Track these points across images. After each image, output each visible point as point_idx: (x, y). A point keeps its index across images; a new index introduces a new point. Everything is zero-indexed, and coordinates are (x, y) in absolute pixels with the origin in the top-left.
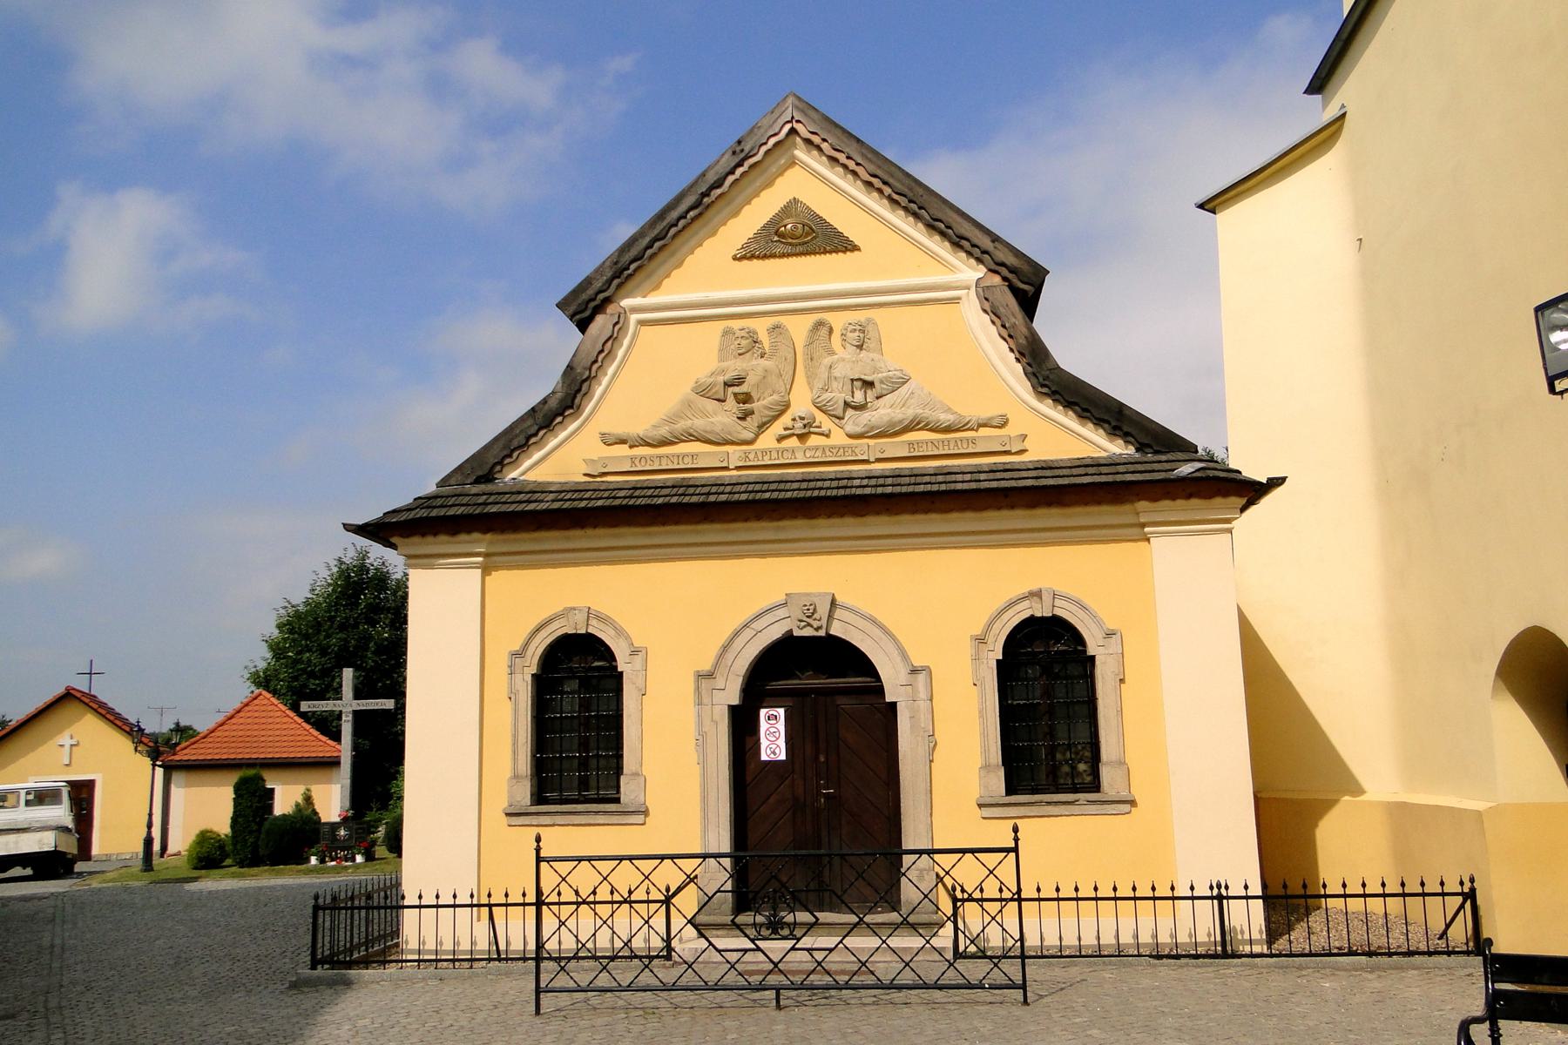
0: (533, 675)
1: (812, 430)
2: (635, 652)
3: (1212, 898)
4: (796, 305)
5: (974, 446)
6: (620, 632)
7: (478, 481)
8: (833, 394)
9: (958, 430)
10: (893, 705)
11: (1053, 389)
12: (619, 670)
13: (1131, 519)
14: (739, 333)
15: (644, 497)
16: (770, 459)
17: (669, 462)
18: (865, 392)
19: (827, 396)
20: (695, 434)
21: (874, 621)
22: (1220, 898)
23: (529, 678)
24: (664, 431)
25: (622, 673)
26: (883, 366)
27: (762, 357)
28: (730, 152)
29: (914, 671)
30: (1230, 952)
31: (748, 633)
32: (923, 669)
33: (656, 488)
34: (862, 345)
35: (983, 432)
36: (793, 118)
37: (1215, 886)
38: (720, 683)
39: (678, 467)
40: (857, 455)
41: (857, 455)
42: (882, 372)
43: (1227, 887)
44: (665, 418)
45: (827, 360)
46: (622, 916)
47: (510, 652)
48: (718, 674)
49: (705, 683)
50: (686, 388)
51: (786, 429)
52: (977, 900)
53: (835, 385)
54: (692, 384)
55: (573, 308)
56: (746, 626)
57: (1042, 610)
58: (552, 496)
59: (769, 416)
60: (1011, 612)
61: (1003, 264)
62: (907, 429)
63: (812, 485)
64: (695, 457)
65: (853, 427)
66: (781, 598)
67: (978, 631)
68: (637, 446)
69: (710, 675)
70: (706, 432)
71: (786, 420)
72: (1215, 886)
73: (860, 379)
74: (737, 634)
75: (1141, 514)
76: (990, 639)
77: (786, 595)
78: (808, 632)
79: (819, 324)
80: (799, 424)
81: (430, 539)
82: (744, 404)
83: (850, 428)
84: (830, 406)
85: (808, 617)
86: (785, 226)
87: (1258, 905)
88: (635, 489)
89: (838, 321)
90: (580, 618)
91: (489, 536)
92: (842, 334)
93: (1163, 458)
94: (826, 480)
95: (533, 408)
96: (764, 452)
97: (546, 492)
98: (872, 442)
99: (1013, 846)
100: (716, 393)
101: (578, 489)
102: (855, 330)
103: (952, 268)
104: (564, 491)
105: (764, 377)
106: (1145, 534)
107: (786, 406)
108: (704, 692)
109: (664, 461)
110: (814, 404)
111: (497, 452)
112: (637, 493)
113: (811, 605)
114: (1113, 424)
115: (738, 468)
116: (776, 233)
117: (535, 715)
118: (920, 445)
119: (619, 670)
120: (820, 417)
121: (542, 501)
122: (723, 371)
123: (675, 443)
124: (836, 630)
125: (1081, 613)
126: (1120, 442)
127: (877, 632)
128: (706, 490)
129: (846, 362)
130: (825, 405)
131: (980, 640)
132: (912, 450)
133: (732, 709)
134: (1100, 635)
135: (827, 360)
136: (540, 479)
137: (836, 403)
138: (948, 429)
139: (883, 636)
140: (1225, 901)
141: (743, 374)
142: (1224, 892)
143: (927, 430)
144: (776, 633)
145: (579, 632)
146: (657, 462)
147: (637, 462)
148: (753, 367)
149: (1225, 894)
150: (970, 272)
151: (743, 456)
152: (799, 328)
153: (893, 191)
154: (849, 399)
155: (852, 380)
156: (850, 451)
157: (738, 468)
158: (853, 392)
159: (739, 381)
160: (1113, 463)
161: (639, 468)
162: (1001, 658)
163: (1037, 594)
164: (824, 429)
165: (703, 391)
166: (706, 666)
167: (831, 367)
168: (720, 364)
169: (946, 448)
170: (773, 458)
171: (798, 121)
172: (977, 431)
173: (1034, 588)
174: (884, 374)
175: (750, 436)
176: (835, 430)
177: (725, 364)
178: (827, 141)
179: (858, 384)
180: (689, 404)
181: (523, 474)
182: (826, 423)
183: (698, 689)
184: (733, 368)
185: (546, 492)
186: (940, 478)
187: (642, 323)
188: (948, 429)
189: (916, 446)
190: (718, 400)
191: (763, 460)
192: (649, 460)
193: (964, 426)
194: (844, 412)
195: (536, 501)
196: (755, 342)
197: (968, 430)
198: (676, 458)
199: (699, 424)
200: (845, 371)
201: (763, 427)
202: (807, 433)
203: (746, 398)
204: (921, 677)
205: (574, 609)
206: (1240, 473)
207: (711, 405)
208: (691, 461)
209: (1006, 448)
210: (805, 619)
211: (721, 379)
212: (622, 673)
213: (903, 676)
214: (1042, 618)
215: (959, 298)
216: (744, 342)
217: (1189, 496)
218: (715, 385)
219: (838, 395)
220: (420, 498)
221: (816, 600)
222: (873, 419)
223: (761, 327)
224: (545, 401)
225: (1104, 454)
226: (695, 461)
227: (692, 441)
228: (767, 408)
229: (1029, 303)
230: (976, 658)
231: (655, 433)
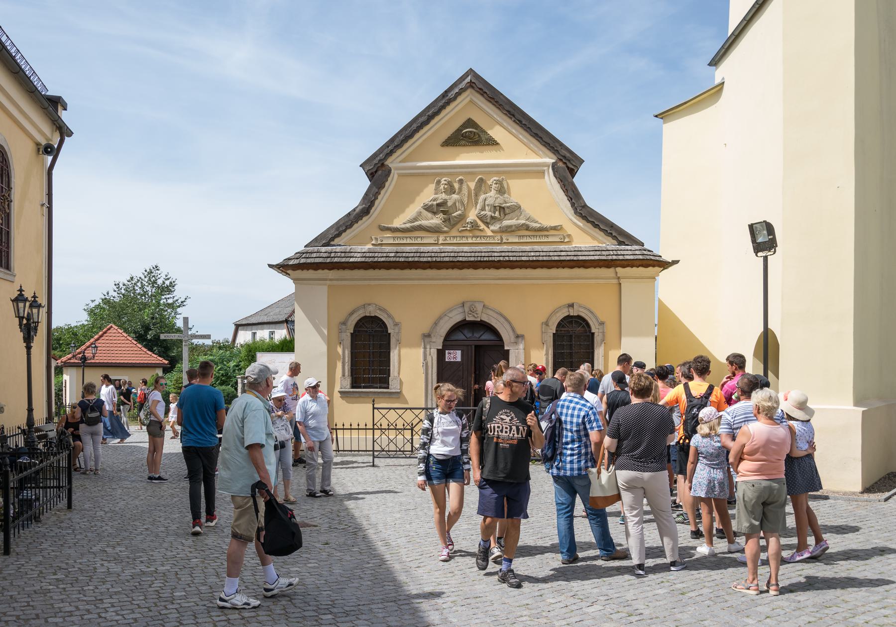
2: (396, 324)
4: (470, 171)
6: (389, 316)
7: (323, 246)
12: (389, 332)
19: (483, 213)
21: (502, 315)
23: (349, 335)
24: (408, 225)
25: (390, 334)
28: (442, 96)
29: (518, 337)
31: (446, 318)
38: (434, 339)
46: (392, 434)
48: (432, 335)
49: (427, 340)
53: (487, 208)
54: (422, 205)
55: (368, 168)
57: (573, 313)
61: (564, 157)
63: (477, 254)
67: (545, 320)
74: (440, 318)
79: (481, 181)
95: (349, 213)
110: (478, 217)
111: (333, 232)
112: (398, 255)
115: (442, 244)
119: (389, 332)
120: (480, 223)
122: (434, 200)
124: (485, 319)
125: (590, 315)
127: (502, 320)
128: (429, 255)
129: (492, 196)
131: (546, 324)
150: (550, 159)
154: (493, 215)
159: (443, 204)
163: (571, 306)
172: (548, 231)
173: (570, 302)
177: (437, 196)
180: (420, 214)
182: (482, 226)
184: (440, 198)
186: (532, 254)
199: (424, 223)
207: (430, 215)
211: (435, 203)
212: (390, 334)
213: (513, 339)
220: (299, 253)
224: (354, 210)
228: (455, 217)
229: (573, 173)
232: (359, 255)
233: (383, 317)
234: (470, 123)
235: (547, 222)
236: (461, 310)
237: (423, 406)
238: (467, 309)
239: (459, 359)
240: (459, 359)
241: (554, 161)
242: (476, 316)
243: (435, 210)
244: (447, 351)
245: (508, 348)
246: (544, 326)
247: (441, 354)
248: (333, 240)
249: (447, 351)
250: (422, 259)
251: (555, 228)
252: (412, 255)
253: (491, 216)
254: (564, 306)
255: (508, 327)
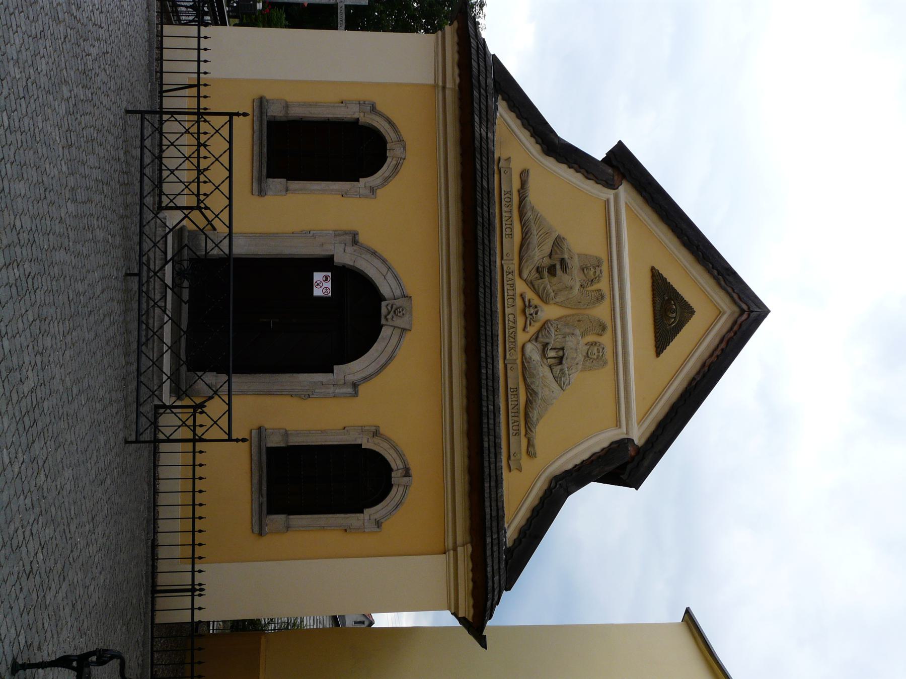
0: (358, 119)
1: (529, 320)
2: (373, 190)
3: (193, 584)
4: (618, 312)
5: (514, 434)
6: (386, 180)
8: (553, 335)
9: (526, 423)
10: (332, 371)
11: (553, 491)
13: (460, 540)
14: (598, 270)
15: (482, 198)
16: (508, 290)
17: (507, 218)
18: (555, 358)
20: (527, 236)
21: (391, 358)
22: (193, 590)
23: (356, 116)
25: (358, 181)
26: (573, 371)
27: (582, 286)
29: (355, 386)
30: (156, 595)
31: (384, 270)
32: (356, 394)
33: (489, 208)
34: (588, 357)
35: (524, 442)
36: (752, 312)
37: (202, 587)
38: (349, 249)
39: (504, 225)
40: (509, 351)
41: (509, 351)
42: (568, 370)
43: (200, 595)
44: (539, 216)
45: (578, 332)
46: (187, 176)
47: (375, 103)
48: (355, 248)
49: (348, 238)
50: (560, 229)
51: (529, 301)
52: (198, 178)
54: (563, 235)
56: (389, 268)
58: (484, 134)
59: (539, 288)
60: (395, 455)
61: (643, 458)
62: (528, 387)
64: (510, 236)
65: (529, 349)
66: (409, 291)
67: (382, 431)
68: (519, 196)
69: (355, 242)
70: (528, 244)
71: (536, 301)
72: (202, 587)
73: (564, 355)
74: (384, 261)
75: (462, 548)
76: (377, 440)
77: (411, 297)
78: (384, 311)
79: (603, 328)
80: (532, 311)
81: (456, 48)
82: (548, 272)
83: (529, 347)
84: (545, 335)
85: (395, 312)
86: (675, 305)
87: (186, 617)
88: (489, 193)
89: (606, 339)
90: (398, 152)
91: (457, 88)
92: (596, 343)
93: (503, 566)
94: (492, 328)
96: (513, 286)
97: (487, 131)
98: (519, 362)
99: (233, 438)
100: (556, 251)
101: (489, 153)
102: (599, 352)
103: (640, 422)
104: (487, 141)
105: (567, 287)
106: (449, 551)
107: (546, 302)
108: (343, 237)
109: (508, 215)
112: (485, 194)
113: (403, 314)
114: (527, 532)
115: (502, 266)
116: (670, 299)
117: (331, 120)
118: (516, 396)
121: (480, 127)
123: (521, 221)
124: (385, 332)
125: (394, 503)
126: (515, 536)
127: (383, 360)
130: (545, 329)
131: (376, 433)
132: (512, 390)
133: (331, 258)
134: (377, 516)
135: (578, 332)
136: (497, 127)
137: (547, 336)
138: (527, 416)
139: (380, 365)
140: (190, 594)
141: (568, 271)
142: (197, 593)
143: (527, 401)
144: (384, 290)
145: (388, 151)
146: (508, 209)
147: (508, 195)
148: (574, 279)
149: (196, 593)
150: (638, 434)
151: (510, 271)
152: (601, 312)
153: (698, 381)
155: (563, 349)
156: (512, 346)
157: (502, 266)
158: (555, 349)
160: (500, 529)
161: (503, 197)
162: (363, 447)
163: (407, 473)
164: (529, 328)
165: (558, 242)
166: (361, 238)
167: (573, 334)
168: (577, 256)
169: (513, 414)
170: (509, 291)
171: (749, 315)
172: (525, 435)
173: (413, 472)
174: (567, 372)
175: (525, 276)
176: (526, 337)
177: (576, 259)
178: (734, 335)
179: (561, 353)
181: (501, 115)
182: (532, 330)
183: (346, 233)
185: (487, 131)
187: (607, 202)
188: (527, 416)
189: (515, 393)
190: (551, 254)
191: (507, 284)
192: (508, 204)
193: (528, 427)
194: (541, 342)
195: (481, 122)
196: (592, 281)
197: (526, 431)
198: (510, 223)
199: (535, 239)
200: (570, 343)
201: (531, 285)
202: (526, 316)
203: (552, 270)
204: (350, 390)
205: (404, 148)
206: (490, 619)
207: (547, 248)
208: (507, 233)
209: (512, 458)
210: (393, 310)
211: (566, 256)
212: (358, 181)
213: (351, 378)
214: (390, 477)
215: (620, 427)
216: (592, 273)
217: (474, 580)
218: (562, 252)
219: (554, 339)
221: (406, 318)
222: (534, 362)
223: (603, 285)
225: (506, 526)
226: (507, 236)
227: (522, 234)
228: (544, 288)
230: (362, 430)
231: (529, 208)
232: (484, 134)
233: (384, 171)
234: (687, 311)
235: (542, 432)
236: (398, 293)
237: (234, 230)
238: (398, 303)
239: (317, 292)
240: (317, 292)
241: (636, 442)
242: (389, 317)
243: (555, 256)
244: (329, 274)
245: (335, 371)
246: (373, 429)
247: (325, 263)
248: (503, 99)
249: (329, 274)
250: (480, 228)
251: (530, 444)
252: (486, 214)
253: (547, 344)
254: (404, 461)
255: (371, 370)
